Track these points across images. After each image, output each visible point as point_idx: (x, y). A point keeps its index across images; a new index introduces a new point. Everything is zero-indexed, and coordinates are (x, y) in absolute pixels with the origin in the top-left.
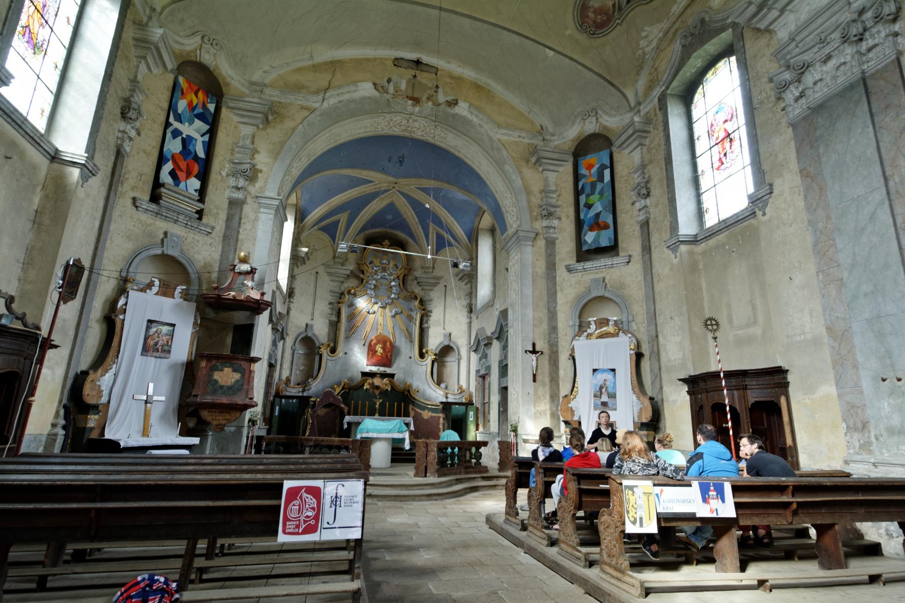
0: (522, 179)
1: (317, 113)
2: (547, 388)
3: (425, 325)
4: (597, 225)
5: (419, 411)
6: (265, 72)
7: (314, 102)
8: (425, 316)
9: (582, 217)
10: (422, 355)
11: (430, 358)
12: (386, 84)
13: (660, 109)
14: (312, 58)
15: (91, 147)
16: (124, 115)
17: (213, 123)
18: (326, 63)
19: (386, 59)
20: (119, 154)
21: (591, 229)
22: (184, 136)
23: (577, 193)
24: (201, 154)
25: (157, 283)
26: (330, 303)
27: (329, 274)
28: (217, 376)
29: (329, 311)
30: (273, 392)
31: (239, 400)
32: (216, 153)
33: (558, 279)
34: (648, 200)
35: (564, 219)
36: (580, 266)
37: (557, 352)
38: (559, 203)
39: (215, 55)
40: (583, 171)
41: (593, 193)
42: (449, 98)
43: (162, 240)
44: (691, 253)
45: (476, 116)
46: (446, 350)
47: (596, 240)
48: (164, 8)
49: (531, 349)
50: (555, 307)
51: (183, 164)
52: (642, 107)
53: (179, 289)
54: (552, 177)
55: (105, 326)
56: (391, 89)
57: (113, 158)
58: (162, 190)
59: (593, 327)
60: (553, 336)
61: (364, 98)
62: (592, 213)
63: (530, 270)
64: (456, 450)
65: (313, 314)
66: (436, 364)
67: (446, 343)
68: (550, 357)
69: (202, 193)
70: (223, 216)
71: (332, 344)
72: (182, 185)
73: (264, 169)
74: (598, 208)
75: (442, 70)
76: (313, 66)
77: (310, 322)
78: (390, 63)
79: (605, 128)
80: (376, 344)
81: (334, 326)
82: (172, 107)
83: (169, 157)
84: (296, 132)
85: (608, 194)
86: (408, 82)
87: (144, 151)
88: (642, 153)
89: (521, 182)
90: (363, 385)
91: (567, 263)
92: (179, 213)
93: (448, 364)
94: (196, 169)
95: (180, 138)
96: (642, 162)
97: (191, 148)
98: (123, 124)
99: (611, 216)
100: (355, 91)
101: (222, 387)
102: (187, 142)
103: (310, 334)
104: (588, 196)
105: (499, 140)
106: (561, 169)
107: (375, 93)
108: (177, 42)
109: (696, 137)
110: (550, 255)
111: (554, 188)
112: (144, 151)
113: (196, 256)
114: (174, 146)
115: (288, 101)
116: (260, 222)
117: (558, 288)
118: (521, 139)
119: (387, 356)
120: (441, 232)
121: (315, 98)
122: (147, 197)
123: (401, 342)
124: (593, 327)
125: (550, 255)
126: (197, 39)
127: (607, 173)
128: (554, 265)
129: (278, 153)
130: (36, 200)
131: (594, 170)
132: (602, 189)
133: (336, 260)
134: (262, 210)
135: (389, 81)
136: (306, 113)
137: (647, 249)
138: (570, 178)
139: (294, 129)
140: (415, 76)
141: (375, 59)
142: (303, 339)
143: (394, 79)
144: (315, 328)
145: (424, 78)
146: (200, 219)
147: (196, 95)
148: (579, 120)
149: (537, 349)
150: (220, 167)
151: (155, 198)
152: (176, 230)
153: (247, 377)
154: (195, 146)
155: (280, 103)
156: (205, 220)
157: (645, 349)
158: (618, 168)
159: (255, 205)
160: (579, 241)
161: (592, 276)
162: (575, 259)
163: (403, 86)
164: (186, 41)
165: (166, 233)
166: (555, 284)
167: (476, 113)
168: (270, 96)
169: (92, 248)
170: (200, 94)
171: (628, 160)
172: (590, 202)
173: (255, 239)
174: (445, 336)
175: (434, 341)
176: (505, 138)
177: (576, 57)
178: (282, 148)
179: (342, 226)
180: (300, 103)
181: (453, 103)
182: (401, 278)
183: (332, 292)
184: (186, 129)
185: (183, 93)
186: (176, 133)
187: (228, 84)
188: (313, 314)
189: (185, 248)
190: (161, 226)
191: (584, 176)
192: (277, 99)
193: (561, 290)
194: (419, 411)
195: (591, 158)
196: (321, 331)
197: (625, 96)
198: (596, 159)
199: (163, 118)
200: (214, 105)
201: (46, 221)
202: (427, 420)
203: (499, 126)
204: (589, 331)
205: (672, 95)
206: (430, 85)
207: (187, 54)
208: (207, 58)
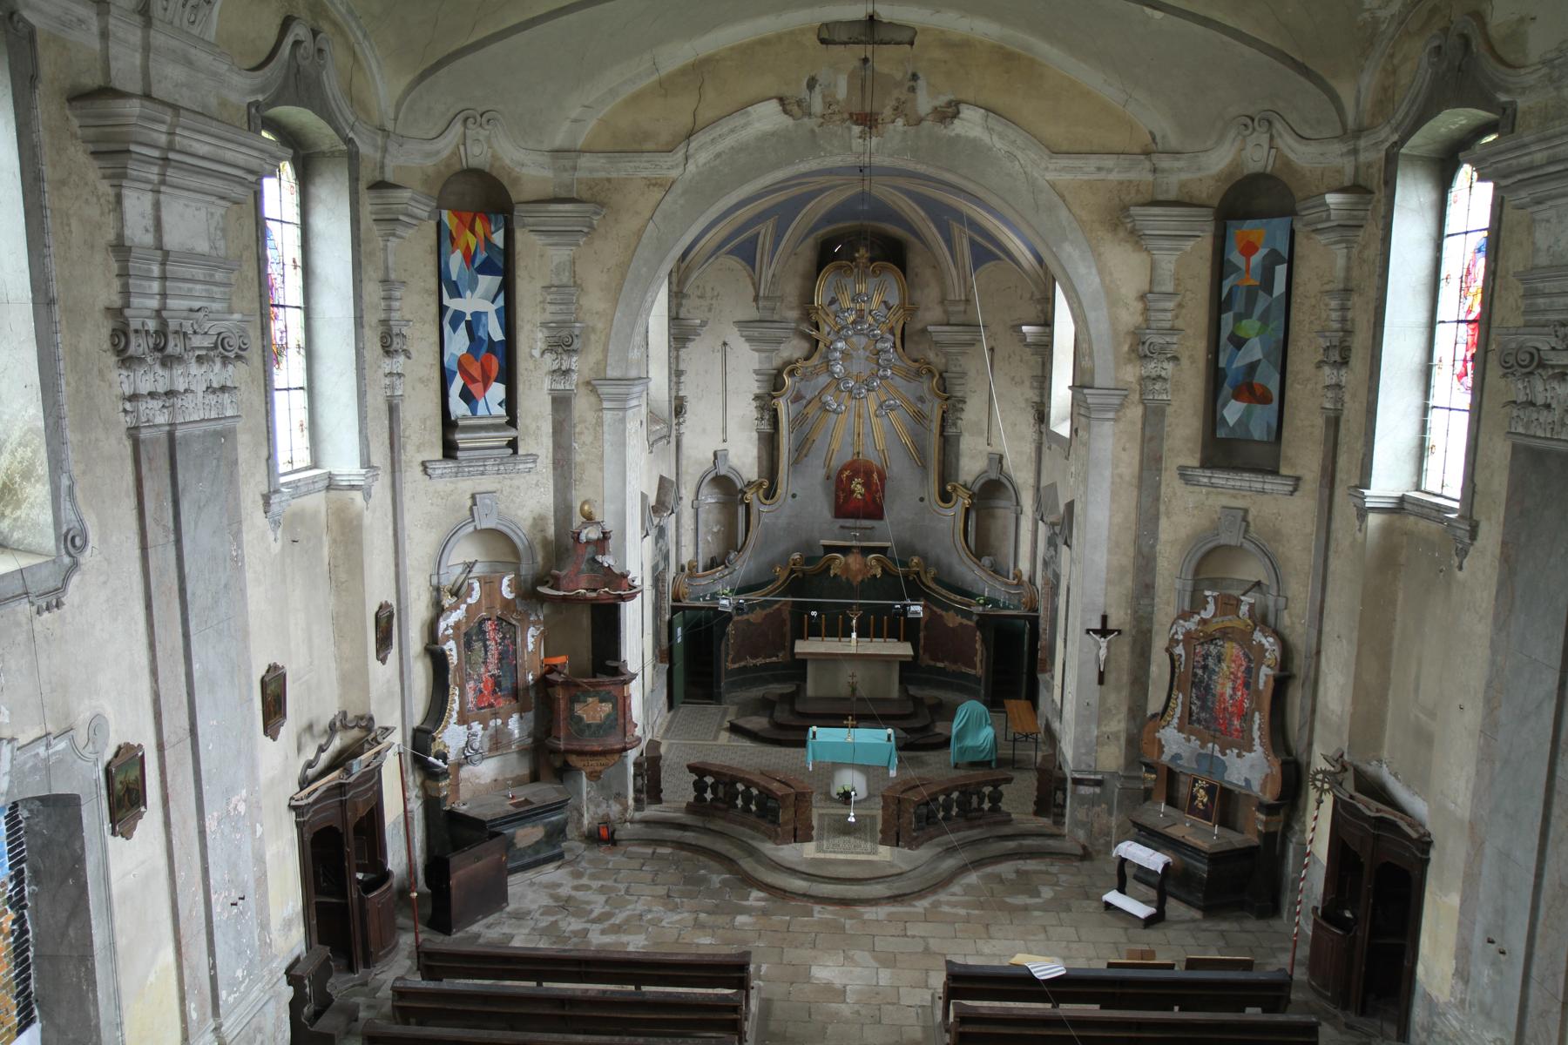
0: (1101, 272)
1: (678, 189)
2: (1125, 693)
3: (951, 431)
4: (1249, 391)
5: (939, 611)
6: (575, 121)
7: (669, 167)
8: (951, 405)
9: (1222, 364)
10: (945, 497)
11: (963, 501)
12: (804, 93)
13: (1386, 183)
14: (655, 67)
15: (366, 463)
16: (388, 351)
17: (503, 266)
18: (683, 72)
19: (802, 31)
20: (393, 410)
21: (1237, 396)
22: (468, 318)
23: (1219, 305)
24: (498, 335)
25: (477, 585)
26: (757, 397)
27: (749, 339)
28: (579, 710)
29: (755, 414)
30: (668, 603)
31: (614, 742)
32: (519, 323)
33: (1163, 489)
34: (1343, 372)
35: (1185, 362)
36: (1204, 476)
37: (1150, 631)
38: (1179, 324)
39: (488, 139)
40: (1235, 257)
41: (1247, 314)
42: (942, 100)
43: (471, 509)
44: (1387, 531)
45: (1001, 136)
46: (993, 489)
47: (1243, 422)
48: (398, 106)
49: (1098, 627)
50: (1153, 547)
51: (475, 371)
52: (1362, 143)
53: (506, 581)
54: (1168, 263)
55: (428, 661)
56: (817, 106)
57: (387, 422)
58: (458, 436)
59: (1211, 607)
60: (1144, 602)
61: (763, 138)
62: (1242, 360)
63: (1107, 473)
64: (955, 795)
65: (724, 430)
66: (973, 515)
67: (993, 476)
68: (1135, 641)
69: (510, 403)
70: (547, 427)
71: (766, 484)
72: (481, 403)
73: (600, 326)
74: (1254, 351)
75: (925, 30)
76: (660, 83)
77: (721, 446)
78: (812, 39)
79: (1287, 163)
80: (850, 479)
81: (769, 442)
82: (442, 275)
83: (455, 367)
84: (644, 240)
85: (1277, 323)
86: (852, 76)
87: (421, 380)
88: (1349, 258)
89: (1097, 280)
90: (829, 568)
91: (1183, 461)
92: (485, 459)
93: (999, 512)
94: (495, 365)
95: (463, 325)
96: (1347, 279)
97: (481, 333)
98: (387, 361)
99: (1277, 377)
100: (744, 127)
101: (589, 726)
102: (473, 326)
103: (723, 471)
104: (1238, 318)
105: (1053, 186)
106: (1189, 245)
107: (787, 121)
108: (428, 155)
109: (1443, 275)
110: (1151, 439)
111: (1169, 288)
112: (421, 380)
113: (520, 513)
114: (458, 343)
115: (623, 174)
116: (606, 428)
117: (1162, 508)
118: (1102, 175)
119: (874, 501)
120: (979, 239)
121: (669, 160)
122: (438, 454)
123: (901, 471)
124: (1211, 607)
125: (1151, 439)
126: (457, 128)
127: (1281, 271)
128: (1159, 459)
129: (620, 288)
130: (326, 551)
131: (1256, 259)
132: (1267, 311)
133: (761, 304)
134: (606, 405)
135: (811, 84)
136: (657, 194)
137: (1329, 476)
138: (1204, 270)
139: (639, 234)
140: (865, 60)
141: (779, 37)
142: (713, 479)
143: (823, 76)
144: (730, 456)
145: (887, 60)
146: (515, 452)
147: (473, 231)
148: (1232, 134)
149: (1111, 625)
150: (531, 342)
151: (450, 450)
152: (486, 483)
153: (622, 705)
154: (486, 326)
155: (609, 180)
156: (521, 451)
157: (1300, 665)
158: (1303, 273)
159: (593, 399)
160: (1212, 417)
161: (1225, 501)
162: (1198, 456)
163: (842, 92)
164: (440, 144)
165: (473, 497)
166: (1157, 499)
167: (999, 128)
168: (591, 170)
169: (393, 568)
170: (479, 226)
171: (1321, 261)
172: (1241, 334)
173: (602, 458)
174: (990, 460)
175: (971, 466)
176: (1068, 177)
177: (1217, 15)
178: (623, 278)
179: (765, 241)
180: (644, 174)
181: (948, 113)
182: (898, 332)
183: (757, 372)
184: (468, 304)
185: (453, 239)
186: (458, 317)
187: (516, 181)
188: (724, 430)
189: (502, 507)
190: (467, 486)
191: (1236, 269)
192: (603, 175)
193: (1168, 515)
194: (939, 611)
195: (1252, 229)
196: (745, 459)
197: (1335, 98)
198: (1265, 234)
199: (434, 309)
200: (501, 232)
201: (343, 577)
202: (953, 629)
203: (1055, 152)
204: (1205, 615)
205: (1412, 159)
206: (899, 76)
207: (448, 166)
208: (477, 155)
